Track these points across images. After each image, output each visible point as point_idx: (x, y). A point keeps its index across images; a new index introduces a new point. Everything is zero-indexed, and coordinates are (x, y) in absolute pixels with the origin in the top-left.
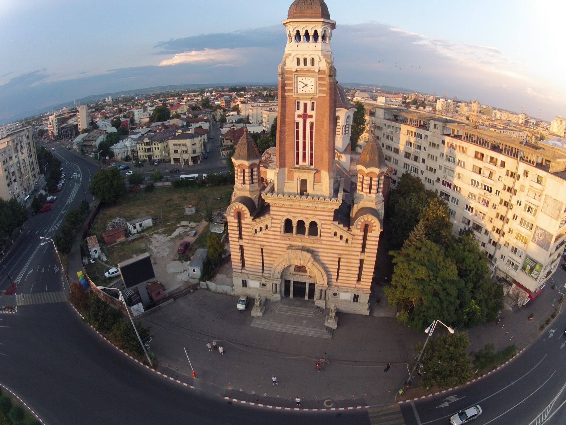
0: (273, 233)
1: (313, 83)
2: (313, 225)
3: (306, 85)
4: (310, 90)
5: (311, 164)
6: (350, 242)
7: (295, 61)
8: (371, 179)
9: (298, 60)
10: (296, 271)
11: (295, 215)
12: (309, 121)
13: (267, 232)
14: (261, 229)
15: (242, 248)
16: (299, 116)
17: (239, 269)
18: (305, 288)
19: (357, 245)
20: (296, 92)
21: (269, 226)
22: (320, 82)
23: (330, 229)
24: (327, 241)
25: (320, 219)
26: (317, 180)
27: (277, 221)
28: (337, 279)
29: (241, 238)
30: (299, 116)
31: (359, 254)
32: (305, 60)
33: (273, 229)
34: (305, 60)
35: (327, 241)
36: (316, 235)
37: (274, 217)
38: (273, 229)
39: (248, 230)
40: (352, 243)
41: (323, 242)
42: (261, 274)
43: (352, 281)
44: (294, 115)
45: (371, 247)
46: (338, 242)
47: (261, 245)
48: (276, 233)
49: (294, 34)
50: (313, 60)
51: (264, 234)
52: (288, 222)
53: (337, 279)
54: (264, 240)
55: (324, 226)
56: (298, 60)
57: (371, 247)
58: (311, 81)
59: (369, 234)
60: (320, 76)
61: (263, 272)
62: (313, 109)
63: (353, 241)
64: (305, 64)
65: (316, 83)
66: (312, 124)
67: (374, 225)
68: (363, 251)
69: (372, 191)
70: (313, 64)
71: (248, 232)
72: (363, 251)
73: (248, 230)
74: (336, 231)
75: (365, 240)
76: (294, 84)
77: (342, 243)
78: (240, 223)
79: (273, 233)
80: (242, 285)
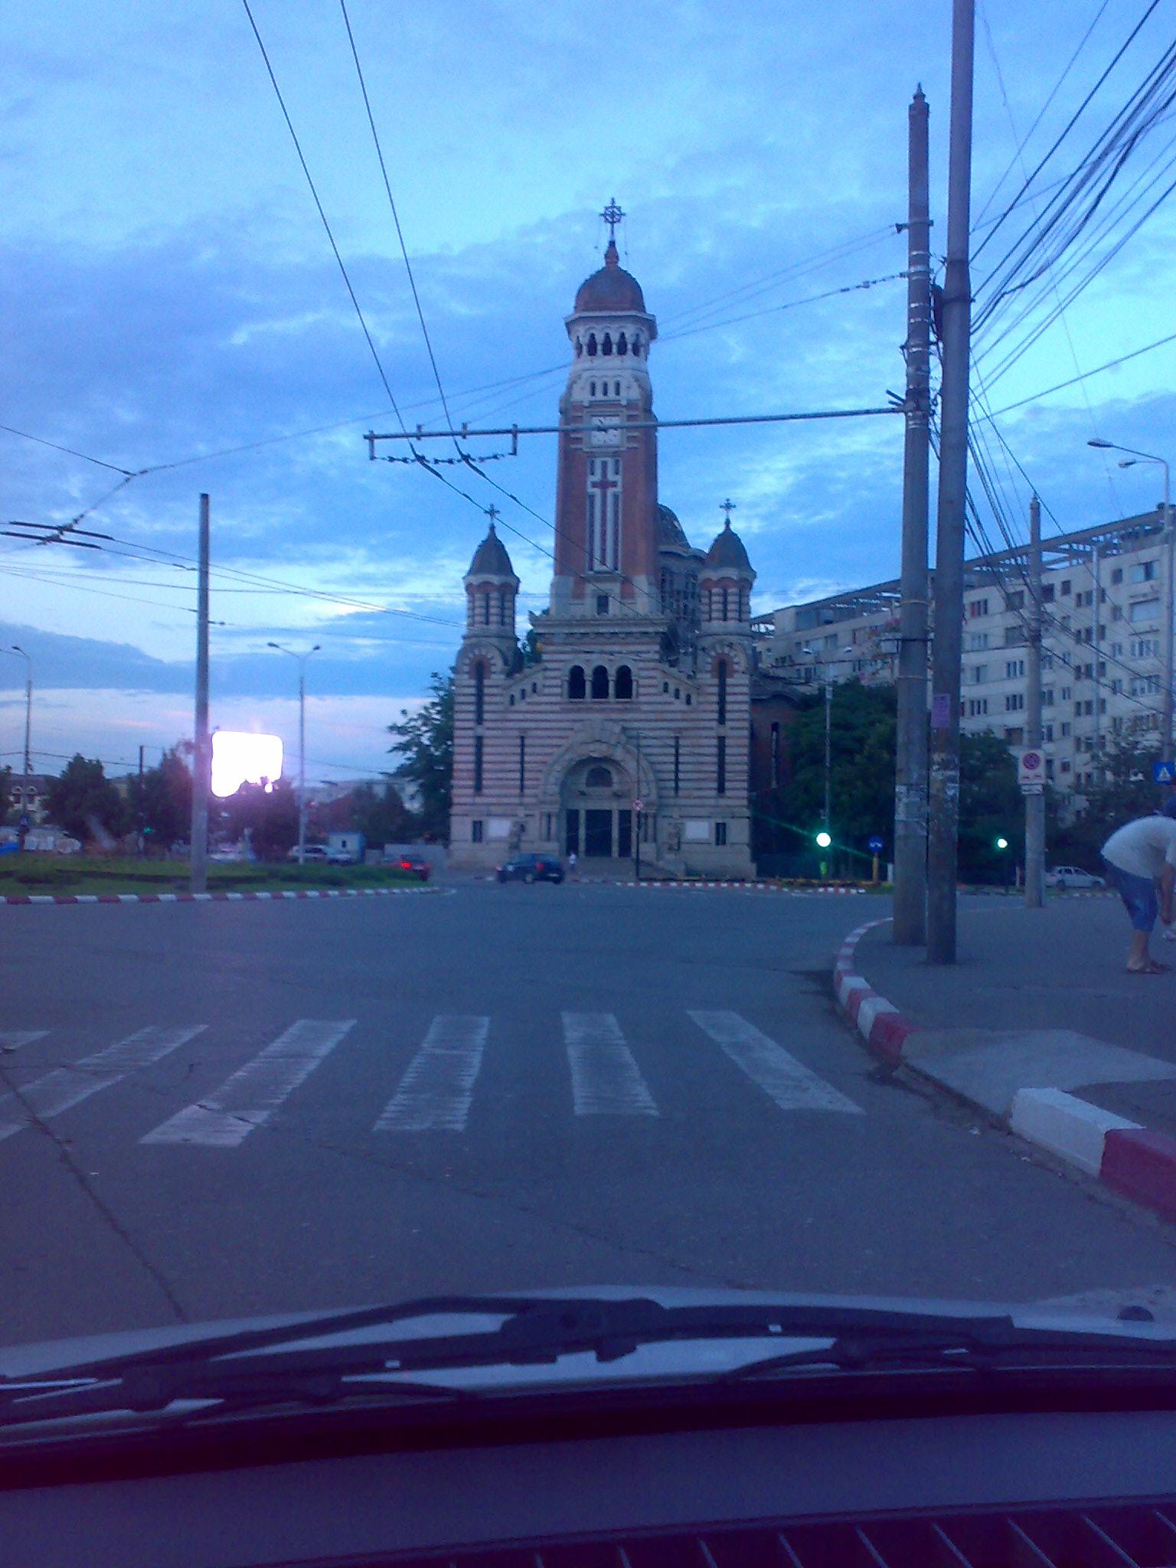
2: (624, 674)
4: (613, 438)
6: (694, 700)
7: (588, 388)
8: (725, 591)
9: (593, 386)
13: (536, 698)
14: (523, 693)
15: (479, 742)
16: (594, 485)
17: (467, 796)
21: (539, 687)
23: (654, 678)
26: (627, 594)
27: (556, 674)
28: (677, 789)
29: (480, 720)
30: (594, 485)
31: (714, 724)
32: (605, 385)
33: (547, 691)
34: (605, 385)
36: (629, 696)
38: (547, 691)
39: (498, 699)
40: (700, 703)
41: (645, 708)
42: (516, 800)
45: (736, 707)
47: (519, 729)
48: (553, 699)
50: (618, 385)
51: (529, 703)
52: (577, 673)
53: (677, 789)
54: (528, 716)
55: (644, 673)
56: (593, 386)
57: (736, 707)
59: (729, 681)
60: (631, 413)
61: (522, 795)
63: (702, 699)
64: (605, 393)
66: (616, 497)
67: (735, 660)
68: (722, 720)
69: (730, 615)
70: (618, 393)
72: (722, 720)
77: (679, 705)
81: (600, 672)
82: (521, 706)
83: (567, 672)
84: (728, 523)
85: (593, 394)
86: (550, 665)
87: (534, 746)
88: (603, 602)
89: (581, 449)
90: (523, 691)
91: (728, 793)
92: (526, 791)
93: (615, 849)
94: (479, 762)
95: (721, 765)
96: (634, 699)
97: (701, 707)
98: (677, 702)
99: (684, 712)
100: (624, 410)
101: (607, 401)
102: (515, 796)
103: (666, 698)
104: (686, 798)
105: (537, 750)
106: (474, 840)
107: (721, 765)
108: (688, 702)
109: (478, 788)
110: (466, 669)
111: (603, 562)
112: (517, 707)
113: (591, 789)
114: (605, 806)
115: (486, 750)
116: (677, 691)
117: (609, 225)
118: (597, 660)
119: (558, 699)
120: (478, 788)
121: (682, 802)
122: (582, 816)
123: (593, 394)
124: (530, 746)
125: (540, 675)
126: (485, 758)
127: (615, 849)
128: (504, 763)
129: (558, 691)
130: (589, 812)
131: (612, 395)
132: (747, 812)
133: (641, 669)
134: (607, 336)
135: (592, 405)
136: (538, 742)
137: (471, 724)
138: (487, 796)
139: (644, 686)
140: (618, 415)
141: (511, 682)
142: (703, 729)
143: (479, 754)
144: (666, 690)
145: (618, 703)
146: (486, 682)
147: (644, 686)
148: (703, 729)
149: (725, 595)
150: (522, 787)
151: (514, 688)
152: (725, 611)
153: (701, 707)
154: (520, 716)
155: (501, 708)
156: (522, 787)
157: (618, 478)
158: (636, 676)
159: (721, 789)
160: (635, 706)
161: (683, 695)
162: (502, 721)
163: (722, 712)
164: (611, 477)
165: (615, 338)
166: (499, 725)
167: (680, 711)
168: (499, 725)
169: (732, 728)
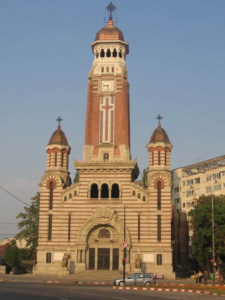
0: (81, 198)
1: (113, 84)
2: (115, 187)
6: (146, 199)
7: (101, 70)
8: (159, 152)
10: (101, 237)
11: (100, 179)
13: (76, 198)
15: (50, 217)
16: (103, 107)
17: (45, 241)
18: (109, 257)
19: (153, 202)
20: (100, 90)
21: (77, 193)
22: (118, 83)
23: (129, 189)
24: (127, 200)
25: (121, 181)
26: (117, 152)
28: (139, 239)
29: (51, 208)
31: (156, 209)
32: (108, 68)
33: (81, 194)
34: (108, 68)
35: (127, 200)
36: (118, 197)
37: (82, 183)
38: (81, 194)
39: (58, 198)
40: (149, 200)
42: (67, 244)
43: (153, 239)
45: (165, 202)
46: (137, 200)
48: (84, 198)
49: (99, 52)
50: (113, 68)
51: (72, 200)
53: (139, 239)
54: (73, 206)
55: (124, 187)
57: (165, 202)
58: (111, 82)
59: (162, 190)
60: (118, 79)
61: (69, 242)
62: (112, 103)
63: (150, 198)
64: (108, 71)
65: (115, 84)
66: (112, 112)
68: (159, 208)
69: (161, 162)
70: (113, 71)
71: (58, 200)
72: (159, 208)
73: (58, 198)
74: (134, 190)
75: (159, 196)
76: (99, 85)
77: (140, 201)
79: (81, 198)
80: (45, 261)
81: (105, 186)
82: (69, 201)
83: (90, 186)
85: (103, 71)
86: (82, 183)
88: (106, 156)
91: (162, 241)
92: (71, 240)
94: (50, 227)
95: (159, 227)
96: (120, 198)
97: (150, 202)
98: (139, 200)
99: (142, 204)
100: (116, 78)
102: (66, 242)
103: (134, 198)
104: (143, 243)
105: (77, 221)
106: (47, 262)
107: (159, 227)
108: (144, 200)
109: (50, 238)
110: (46, 185)
111: (106, 139)
112: (67, 202)
113: (100, 239)
114: (107, 247)
117: (109, 12)
118: (104, 181)
119: (86, 198)
120: (50, 238)
122: (96, 251)
123: (103, 71)
125: (78, 187)
130: (98, 249)
131: (110, 72)
133: (123, 185)
134: (109, 50)
136: (77, 217)
137: (47, 209)
138: (54, 242)
139: (125, 193)
140: (113, 80)
141: (64, 190)
143: (50, 223)
144: (134, 194)
146: (54, 191)
147: (125, 193)
149: (159, 154)
150: (69, 238)
151: (67, 193)
152: (159, 161)
153: (150, 202)
154: (69, 206)
155: (60, 202)
156: (69, 238)
157: (113, 105)
159: (159, 239)
160: (120, 202)
163: (159, 204)
164: (110, 104)
165: (112, 51)
167: (140, 204)
169: (164, 212)
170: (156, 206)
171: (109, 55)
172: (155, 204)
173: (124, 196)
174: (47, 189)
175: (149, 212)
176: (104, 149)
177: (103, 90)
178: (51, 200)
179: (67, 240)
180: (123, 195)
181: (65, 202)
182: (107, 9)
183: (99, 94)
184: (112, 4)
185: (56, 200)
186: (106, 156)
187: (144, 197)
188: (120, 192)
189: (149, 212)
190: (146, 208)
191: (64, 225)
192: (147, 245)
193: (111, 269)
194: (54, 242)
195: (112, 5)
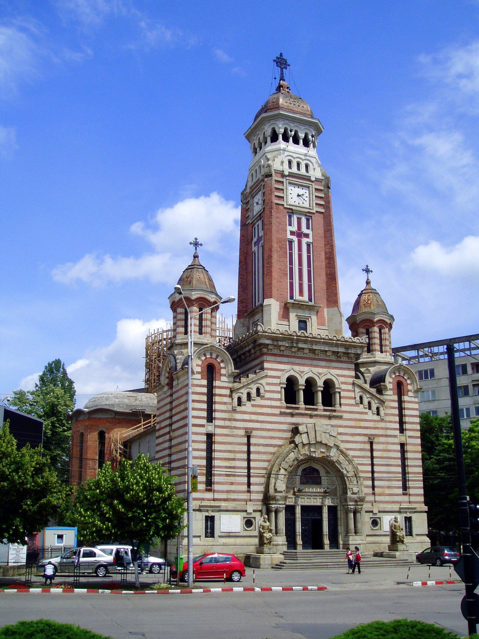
0: (268, 403)
3: (299, 196)
5: (310, 300)
6: (382, 412)
9: (290, 162)
12: (304, 240)
13: (259, 401)
21: (262, 391)
24: (351, 412)
25: (338, 375)
29: (210, 419)
33: (267, 395)
34: (298, 164)
35: (351, 412)
38: (267, 395)
40: (386, 414)
42: (245, 496)
44: (286, 231)
46: (366, 413)
49: (269, 132)
50: (307, 166)
51: (253, 406)
52: (291, 382)
54: (254, 417)
55: (344, 387)
62: (308, 228)
66: (308, 245)
70: (307, 171)
75: (401, 409)
77: (370, 416)
78: (210, 387)
79: (268, 403)
81: (310, 383)
82: (248, 407)
83: (284, 381)
84: (368, 283)
85: (290, 167)
86: (270, 373)
87: (259, 445)
88: (303, 324)
89: (283, 205)
90: (249, 395)
91: (411, 491)
92: (253, 488)
93: (326, 541)
96: (337, 407)
99: (375, 421)
101: (299, 174)
102: (243, 492)
103: (360, 408)
104: (380, 495)
108: (378, 414)
111: (301, 293)
114: (317, 502)
115: (216, 447)
116: (369, 403)
119: (278, 403)
121: (378, 498)
122: (298, 510)
124: (255, 445)
125: (263, 381)
126: (216, 455)
127: (326, 541)
128: (234, 459)
129: (278, 396)
130: (303, 508)
132: (426, 508)
133: (342, 383)
135: (291, 175)
136: (262, 441)
138: (219, 492)
141: (237, 385)
142: (390, 436)
143: (210, 450)
145: (325, 410)
146: (217, 383)
148: (390, 436)
150: (249, 484)
153: (387, 418)
154: (247, 417)
156: (249, 484)
158: (338, 388)
161: (374, 407)
162: (230, 420)
163: (401, 423)
164: (304, 230)
166: (227, 423)
167: (371, 421)
168: (227, 423)
170: (397, 426)
171: (296, 141)
172: (395, 422)
173: (346, 405)
174: (202, 378)
175: (387, 436)
176: (301, 313)
177: (291, 202)
178: (210, 402)
179: (245, 488)
180: (343, 401)
181: (238, 409)
182: (275, 62)
183: (285, 206)
184: (283, 57)
185: (220, 403)
186: (302, 325)
187: (378, 409)
188: (338, 395)
189: (387, 436)
190: (382, 428)
191: (238, 456)
192: (387, 498)
193: (327, 547)
194: (219, 492)
195: (284, 59)
